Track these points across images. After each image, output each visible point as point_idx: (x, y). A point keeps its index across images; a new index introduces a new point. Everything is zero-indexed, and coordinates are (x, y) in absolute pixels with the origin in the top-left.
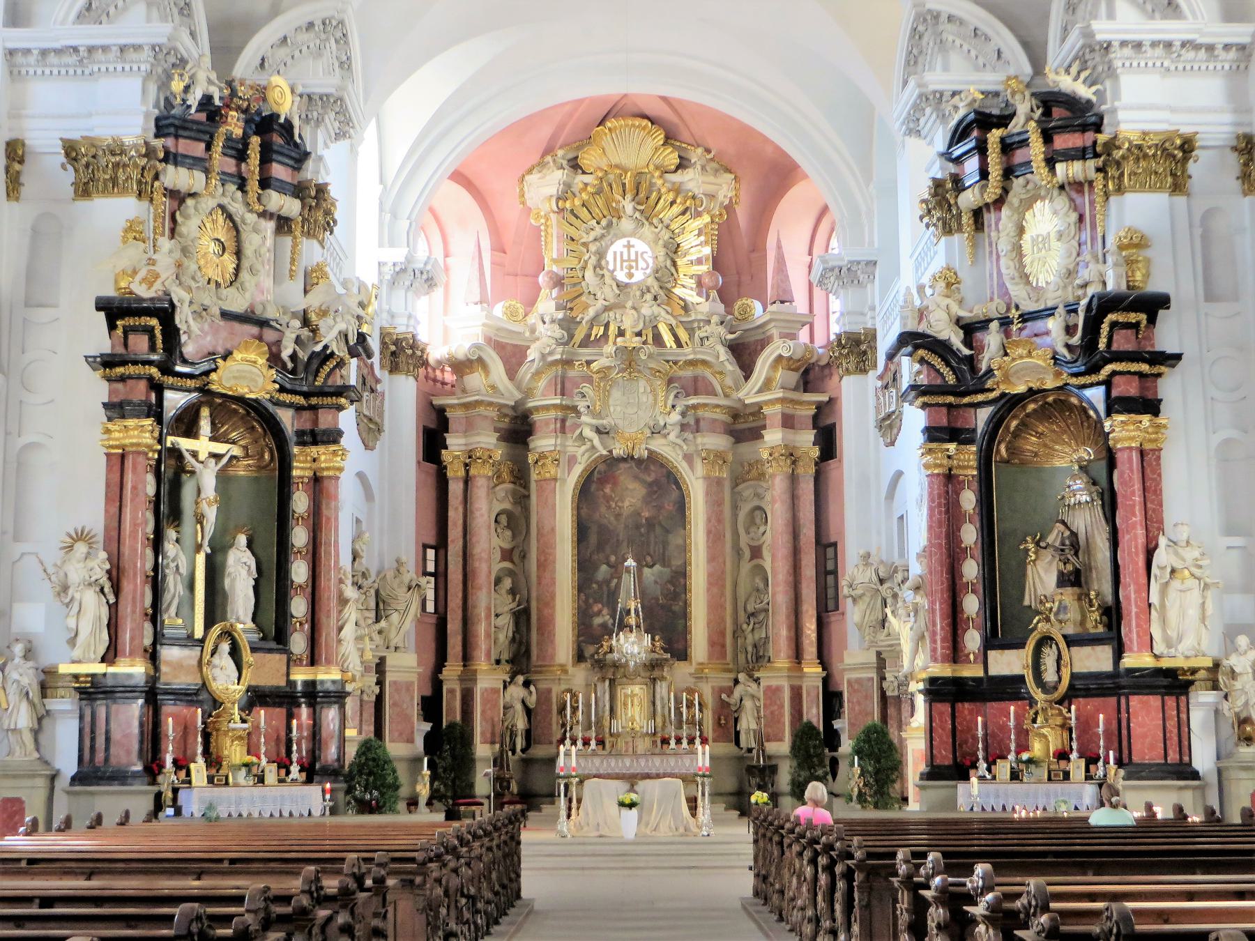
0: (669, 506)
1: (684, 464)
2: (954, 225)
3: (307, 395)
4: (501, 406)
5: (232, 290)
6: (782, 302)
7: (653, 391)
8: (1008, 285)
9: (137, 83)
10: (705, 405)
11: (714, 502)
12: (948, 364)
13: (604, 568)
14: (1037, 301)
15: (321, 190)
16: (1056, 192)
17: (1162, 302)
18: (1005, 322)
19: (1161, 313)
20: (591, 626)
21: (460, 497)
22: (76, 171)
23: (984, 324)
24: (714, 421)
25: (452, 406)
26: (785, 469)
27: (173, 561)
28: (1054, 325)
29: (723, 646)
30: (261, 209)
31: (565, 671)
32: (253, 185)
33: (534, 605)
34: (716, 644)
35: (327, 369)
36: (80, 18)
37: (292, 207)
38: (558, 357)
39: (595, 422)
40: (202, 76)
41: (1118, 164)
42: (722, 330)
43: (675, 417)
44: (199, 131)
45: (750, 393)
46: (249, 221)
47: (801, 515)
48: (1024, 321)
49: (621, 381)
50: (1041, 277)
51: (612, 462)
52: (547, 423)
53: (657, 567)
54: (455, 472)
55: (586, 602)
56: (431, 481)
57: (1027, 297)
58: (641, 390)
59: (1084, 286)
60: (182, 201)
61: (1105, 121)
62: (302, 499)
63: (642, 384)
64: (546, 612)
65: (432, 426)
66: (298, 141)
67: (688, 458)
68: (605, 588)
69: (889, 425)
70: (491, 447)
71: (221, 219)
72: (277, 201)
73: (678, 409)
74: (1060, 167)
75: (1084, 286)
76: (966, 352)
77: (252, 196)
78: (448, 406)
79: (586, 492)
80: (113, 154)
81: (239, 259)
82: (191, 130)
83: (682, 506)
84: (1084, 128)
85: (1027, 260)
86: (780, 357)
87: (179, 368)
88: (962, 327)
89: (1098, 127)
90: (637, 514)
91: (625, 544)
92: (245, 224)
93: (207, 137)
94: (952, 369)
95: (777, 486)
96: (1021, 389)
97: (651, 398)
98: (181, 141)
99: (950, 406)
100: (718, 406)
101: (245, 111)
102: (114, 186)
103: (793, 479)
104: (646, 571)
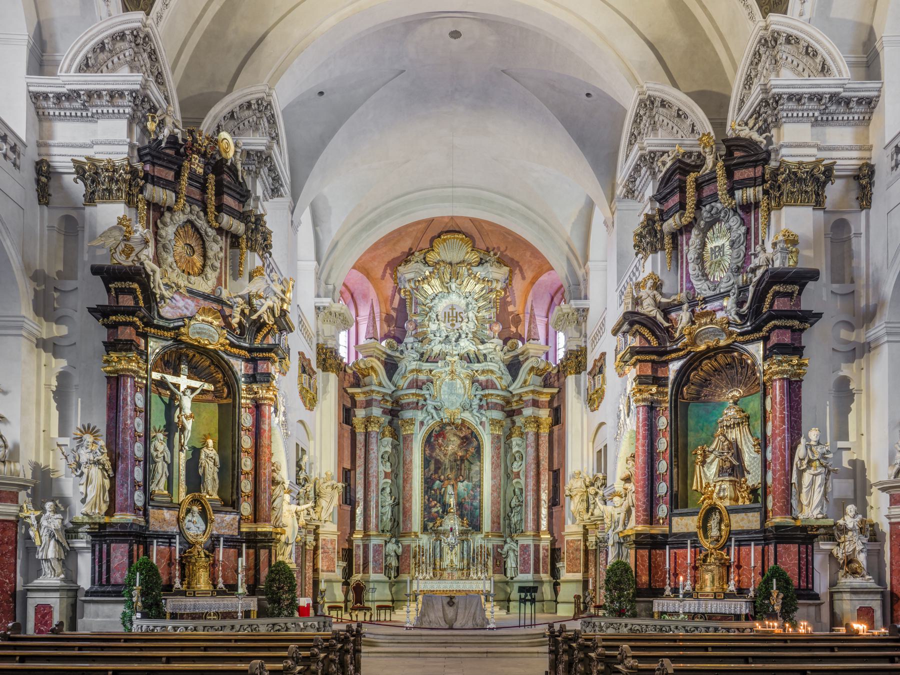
0: (472, 450)
1: (481, 427)
2: (659, 246)
3: (250, 350)
4: (384, 395)
5: (199, 278)
6: (534, 340)
7: (465, 387)
8: (694, 282)
9: (123, 124)
10: (492, 395)
11: (496, 448)
12: (653, 333)
13: (438, 482)
14: (714, 290)
15: (259, 219)
16: (731, 213)
17: (814, 275)
18: (693, 303)
19: (811, 285)
20: (431, 512)
21: (363, 443)
22: (86, 185)
23: (678, 306)
24: (496, 404)
25: (358, 393)
26: (534, 430)
27: (161, 453)
28: (729, 303)
29: (499, 524)
30: (217, 225)
31: (417, 536)
32: (211, 208)
33: (401, 501)
34: (495, 522)
35: (262, 334)
36: (80, 70)
37: (239, 227)
38: (414, 367)
39: (434, 403)
40: (169, 121)
41: (779, 187)
42: (501, 354)
43: (476, 402)
44: (170, 162)
45: (516, 388)
46: (210, 234)
47: (541, 454)
48: (706, 302)
49: (447, 380)
50: (717, 274)
51: (443, 426)
52: (408, 404)
53: (466, 482)
54: (360, 430)
55: (428, 500)
56: (347, 435)
57: (707, 288)
58: (458, 386)
59: (753, 271)
60: (162, 214)
61: (773, 156)
62: (248, 418)
63: (459, 381)
64: (407, 505)
65: (349, 405)
66: (241, 181)
67: (481, 423)
68: (438, 492)
69: (593, 400)
70: (379, 416)
71: (191, 231)
72: (226, 220)
73: (478, 397)
74: (736, 192)
75: (753, 271)
76: (666, 324)
77: (211, 217)
78: (356, 393)
79: (430, 442)
80: (107, 170)
81: (205, 260)
82: (164, 160)
83: (479, 450)
84: (755, 164)
85: (707, 265)
86: (532, 369)
87: (155, 322)
88: (662, 311)
89: (766, 161)
90: (455, 454)
91: (449, 470)
92: (208, 236)
93: (175, 167)
94: (657, 337)
95: (531, 438)
96: (703, 347)
97: (463, 392)
98: (157, 168)
99: (653, 362)
100: (498, 396)
101: (204, 155)
102: (109, 196)
103: (537, 435)
104: (459, 483)
